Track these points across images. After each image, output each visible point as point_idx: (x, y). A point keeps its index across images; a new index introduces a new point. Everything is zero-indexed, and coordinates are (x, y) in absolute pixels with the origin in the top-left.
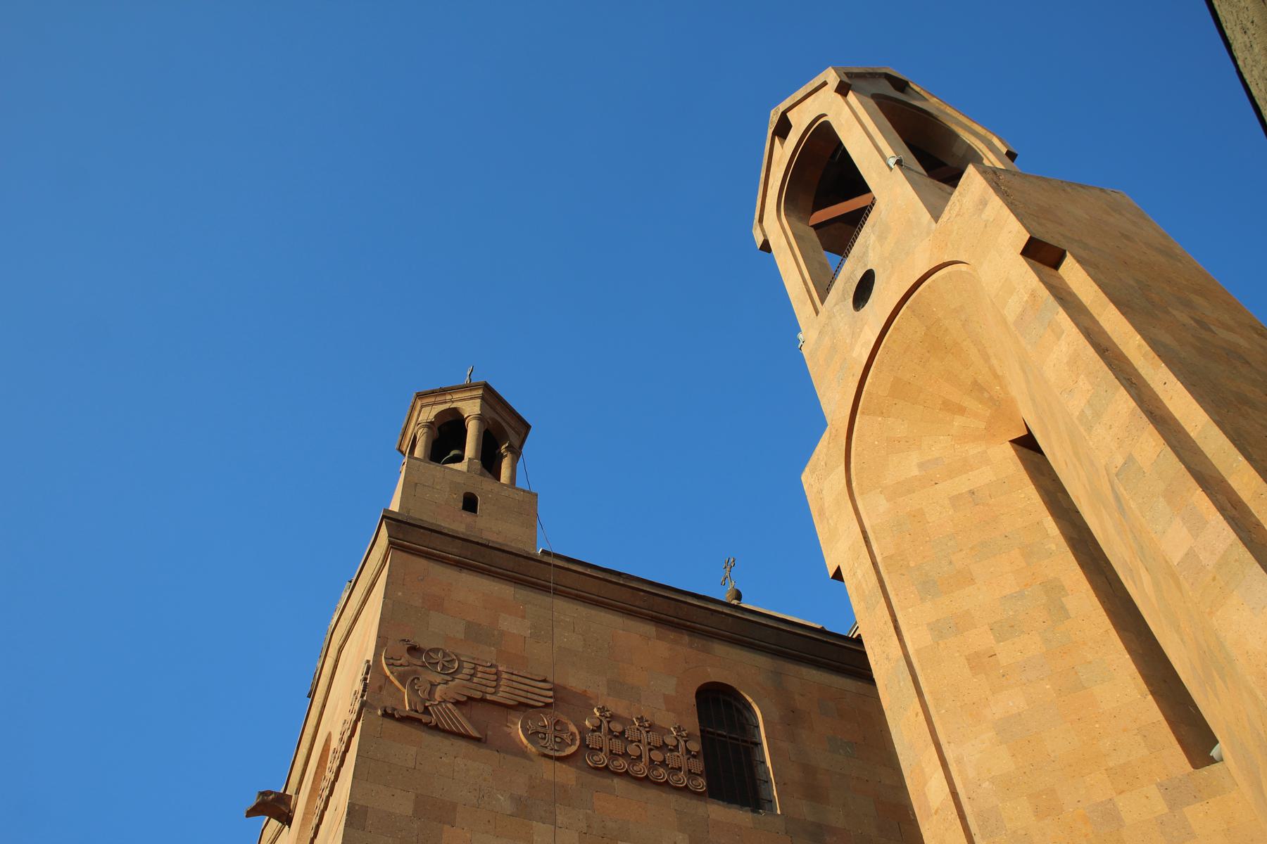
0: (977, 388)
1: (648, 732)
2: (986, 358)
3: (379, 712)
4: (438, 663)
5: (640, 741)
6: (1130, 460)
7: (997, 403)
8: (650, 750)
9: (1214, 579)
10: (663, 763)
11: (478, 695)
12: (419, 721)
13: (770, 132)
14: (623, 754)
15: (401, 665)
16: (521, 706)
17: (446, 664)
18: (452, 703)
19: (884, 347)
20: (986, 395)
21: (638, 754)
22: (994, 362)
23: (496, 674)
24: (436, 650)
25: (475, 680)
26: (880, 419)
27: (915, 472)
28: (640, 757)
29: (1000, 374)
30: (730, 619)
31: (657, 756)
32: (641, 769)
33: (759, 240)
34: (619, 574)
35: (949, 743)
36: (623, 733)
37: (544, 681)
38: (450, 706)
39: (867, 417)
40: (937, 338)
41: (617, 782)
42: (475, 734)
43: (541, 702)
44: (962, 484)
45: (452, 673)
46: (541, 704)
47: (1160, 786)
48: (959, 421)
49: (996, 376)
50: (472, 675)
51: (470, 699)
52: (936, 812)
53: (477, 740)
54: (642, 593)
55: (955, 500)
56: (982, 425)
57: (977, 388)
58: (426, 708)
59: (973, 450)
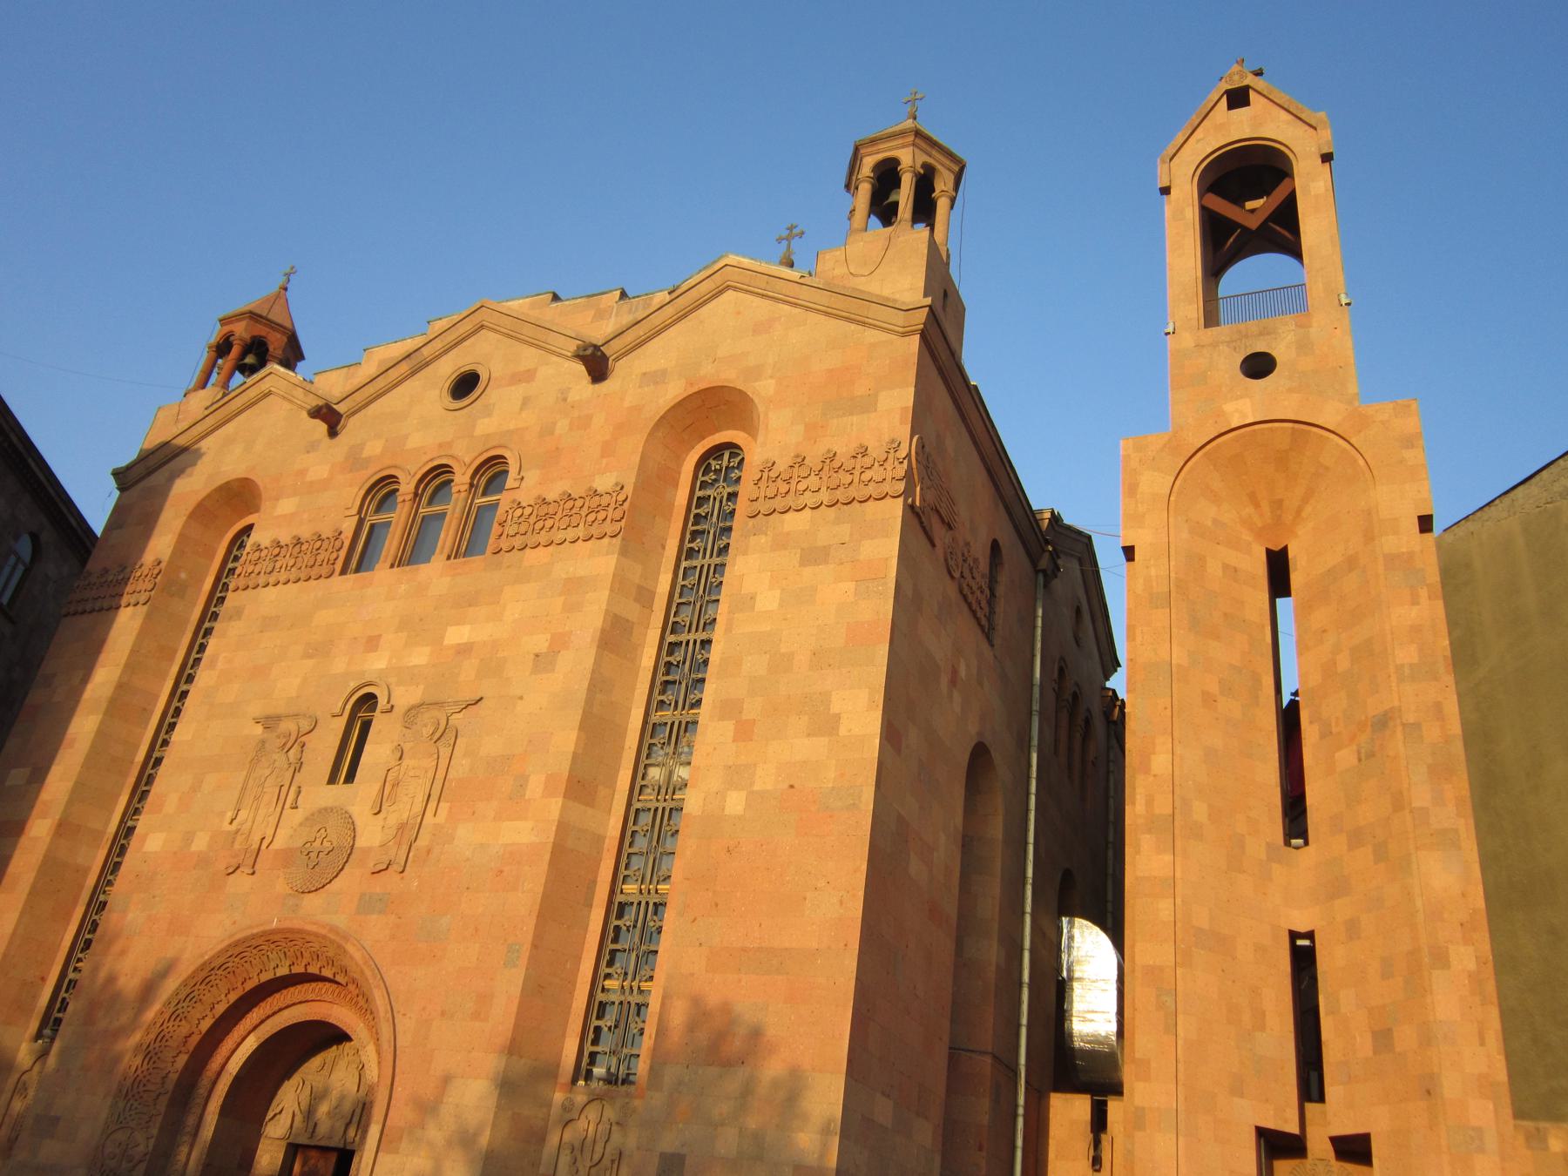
0: (1278, 504)
2: (1306, 500)
6: (1417, 726)
9: (1432, 835)
20: (1279, 512)
22: (1308, 509)
27: (1209, 523)
29: (1304, 514)
34: (993, 426)
35: (1180, 742)
41: (965, 608)
47: (1267, 843)
48: (1250, 510)
49: (1299, 512)
52: (1155, 776)
55: (1226, 567)
56: (1260, 525)
57: (1278, 504)
59: (1247, 536)
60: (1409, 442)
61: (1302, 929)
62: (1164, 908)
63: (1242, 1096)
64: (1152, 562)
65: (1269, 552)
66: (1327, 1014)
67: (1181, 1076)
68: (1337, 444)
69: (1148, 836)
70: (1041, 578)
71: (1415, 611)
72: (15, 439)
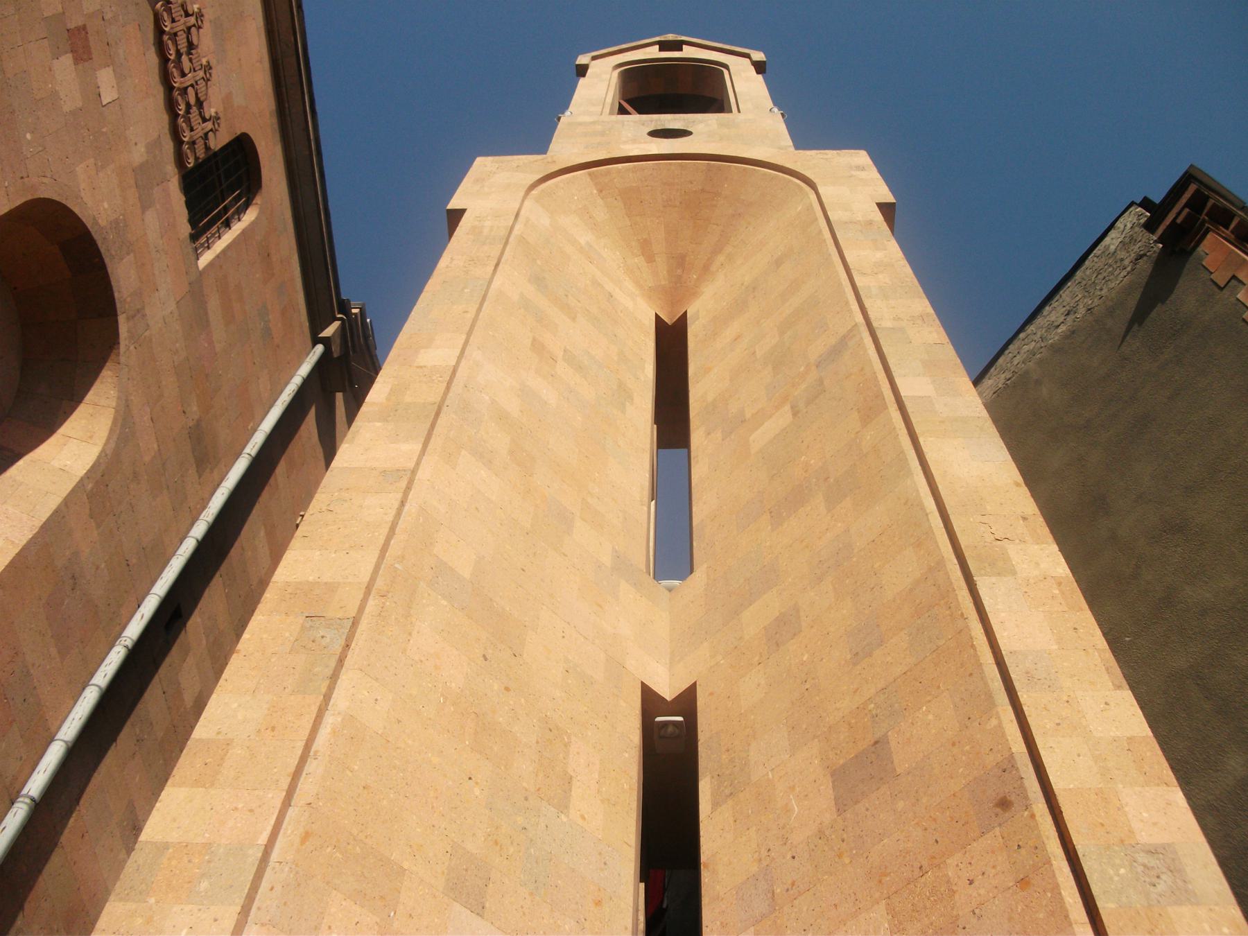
2: (717, 250)
7: (678, 285)
9: (943, 422)
13: (658, 39)
19: (656, 164)
20: (679, 271)
26: (595, 191)
29: (713, 268)
30: (307, 153)
33: (582, 60)
39: (588, 180)
40: (700, 203)
44: (609, 287)
48: (639, 261)
54: (292, 39)
60: (861, 168)
61: (668, 690)
62: (379, 507)
63: (480, 910)
64: (489, 218)
65: (658, 320)
66: (716, 805)
67: (307, 787)
68: (765, 174)
69: (378, 424)
70: (320, 348)
71: (879, 255)
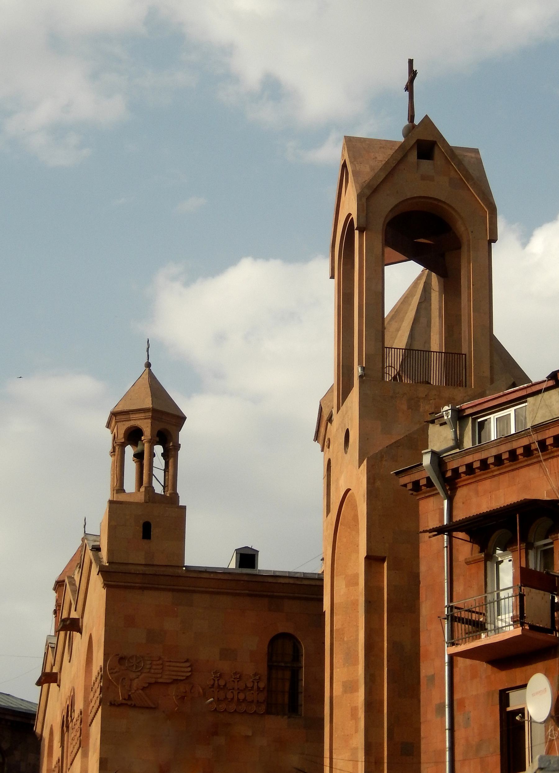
1: (238, 681)
3: (108, 704)
4: (133, 665)
5: (233, 689)
8: (239, 693)
10: (244, 700)
11: (153, 680)
12: (127, 704)
14: (224, 699)
15: (116, 672)
16: (175, 681)
17: (137, 664)
18: (142, 689)
21: (232, 697)
23: (162, 664)
24: (132, 657)
25: (152, 671)
28: (233, 699)
31: (241, 696)
32: (232, 707)
36: (225, 685)
37: (187, 661)
38: (140, 691)
42: (153, 706)
43: (183, 676)
45: (141, 670)
46: (184, 678)
50: (150, 668)
51: (150, 684)
53: (155, 708)
54: (242, 582)
58: (129, 696)
72: (11, 718)
